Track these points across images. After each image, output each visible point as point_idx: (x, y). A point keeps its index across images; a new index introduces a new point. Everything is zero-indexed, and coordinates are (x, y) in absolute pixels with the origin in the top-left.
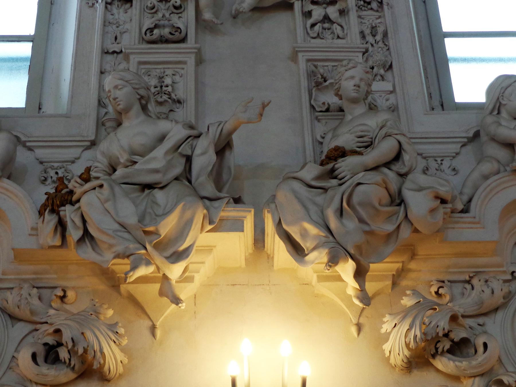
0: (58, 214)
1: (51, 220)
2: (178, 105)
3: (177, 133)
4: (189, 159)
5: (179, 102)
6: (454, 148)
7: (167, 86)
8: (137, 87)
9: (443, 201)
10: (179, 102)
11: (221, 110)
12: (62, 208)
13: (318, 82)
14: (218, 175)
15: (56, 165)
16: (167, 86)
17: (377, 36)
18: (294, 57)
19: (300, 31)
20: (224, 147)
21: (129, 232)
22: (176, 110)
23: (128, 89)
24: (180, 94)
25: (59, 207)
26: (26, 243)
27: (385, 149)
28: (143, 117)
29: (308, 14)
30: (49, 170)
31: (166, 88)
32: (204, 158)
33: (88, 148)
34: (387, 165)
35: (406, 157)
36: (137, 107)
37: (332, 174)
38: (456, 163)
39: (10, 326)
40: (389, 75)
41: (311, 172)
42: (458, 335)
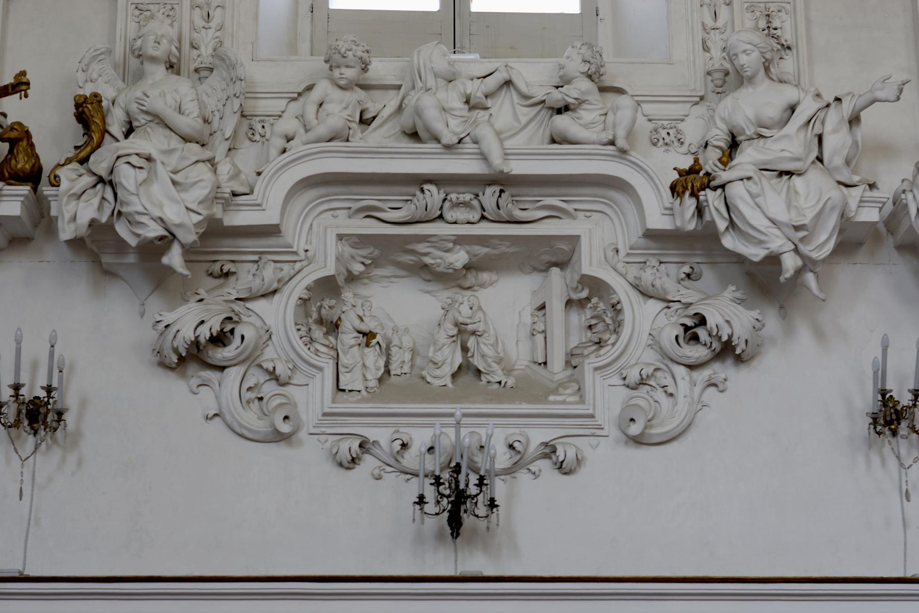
0: (698, 199)
1: (690, 204)
2: (787, 51)
4: (820, 138)
5: (789, 48)
7: (776, 29)
8: (764, 50)
10: (789, 48)
12: (702, 193)
15: (665, 123)
16: (776, 29)
21: (779, 229)
22: (785, 57)
25: (699, 191)
26: (658, 221)
28: (767, 82)
30: (660, 130)
31: (775, 32)
33: (697, 103)
36: (762, 72)
39: (642, 302)
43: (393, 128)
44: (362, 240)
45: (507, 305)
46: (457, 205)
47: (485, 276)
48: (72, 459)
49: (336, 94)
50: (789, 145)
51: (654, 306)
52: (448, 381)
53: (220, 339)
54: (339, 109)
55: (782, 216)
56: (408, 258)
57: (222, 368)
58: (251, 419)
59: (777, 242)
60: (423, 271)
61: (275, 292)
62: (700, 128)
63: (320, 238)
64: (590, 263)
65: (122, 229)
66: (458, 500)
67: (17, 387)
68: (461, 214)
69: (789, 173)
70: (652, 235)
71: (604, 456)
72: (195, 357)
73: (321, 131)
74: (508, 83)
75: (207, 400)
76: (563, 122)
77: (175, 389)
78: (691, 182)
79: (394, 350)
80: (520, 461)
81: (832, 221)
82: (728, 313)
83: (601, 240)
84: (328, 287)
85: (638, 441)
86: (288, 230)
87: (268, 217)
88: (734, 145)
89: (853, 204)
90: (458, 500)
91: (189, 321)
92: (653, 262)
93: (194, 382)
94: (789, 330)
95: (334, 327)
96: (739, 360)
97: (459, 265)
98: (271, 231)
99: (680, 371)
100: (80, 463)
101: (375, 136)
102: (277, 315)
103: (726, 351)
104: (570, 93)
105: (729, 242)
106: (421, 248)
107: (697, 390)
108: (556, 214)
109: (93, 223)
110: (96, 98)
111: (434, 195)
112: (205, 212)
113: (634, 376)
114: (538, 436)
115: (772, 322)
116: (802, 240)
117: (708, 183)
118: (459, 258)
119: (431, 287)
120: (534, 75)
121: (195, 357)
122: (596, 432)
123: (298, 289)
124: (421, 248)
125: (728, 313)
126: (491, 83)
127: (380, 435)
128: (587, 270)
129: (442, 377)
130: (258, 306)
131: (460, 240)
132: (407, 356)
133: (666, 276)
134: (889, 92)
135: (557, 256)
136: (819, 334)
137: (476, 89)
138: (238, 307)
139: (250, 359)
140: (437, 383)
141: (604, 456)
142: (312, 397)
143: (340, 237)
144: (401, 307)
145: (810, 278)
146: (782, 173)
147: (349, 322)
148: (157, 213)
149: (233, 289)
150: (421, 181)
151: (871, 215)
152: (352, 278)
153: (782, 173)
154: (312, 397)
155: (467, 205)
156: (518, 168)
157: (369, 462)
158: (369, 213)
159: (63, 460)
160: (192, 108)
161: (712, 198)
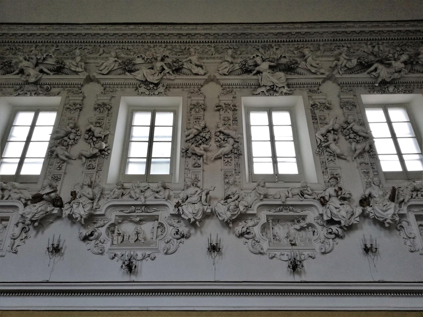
1: (177, 209)
3: (199, 191)
4: (201, 197)
6: (251, 191)
9: (246, 207)
11: (207, 186)
13: (226, 176)
14: (206, 201)
17: (238, 165)
18: (221, 170)
19: (223, 165)
20: (207, 194)
23: (190, 182)
24: (199, 179)
27: (236, 196)
29: (225, 160)
32: (204, 197)
34: (236, 200)
35: (240, 198)
37: (226, 202)
38: (251, 194)
40: (239, 174)
41: (222, 202)
42: (248, 231)
43: (128, 196)
44: (120, 216)
45: (147, 228)
46: (138, 210)
47: (144, 222)
48: (62, 258)
49: (117, 190)
50: (195, 198)
51: (172, 227)
52: (133, 242)
53: (92, 235)
54: (118, 192)
55: (191, 212)
56: (129, 219)
57: (92, 240)
58: (96, 250)
59: (190, 216)
60: (131, 221)
61: (103, 226)
62: (183, 195)
65: (74, 215)
67: (53, 245)
68: (138, 211)
69: (194, 203)
70: (171, 214)
71: (160, 256)
72: (86, 239)
73: (113, 197)
74: (149, 188)
75: (89, 246)
76: (157, 195)
77: (83, 245)
78: (178, 205)
79: (125, 236)
80: (144, 258)
81: (200, 212)
82: (184, 229)
83: (164, 215)
84: (113, 225)
85: (166, 253)
86: (107, 215)
87: (102, 212)
88: (187, 198)
89: (205, 209)
90: (130, 268)
91: (85, 232)
92: (172, 219)
93: (86, 243)
94: (196, 232)
95: (113, 232)
96: (187, 238)
97: (138, 220)
98: (103, 215)
99: (175, 240)
100: (63, 259)
101: (124, 197)
102: (103, 230)
103: (183, 236)
104: (158, 190)
105: (183, 216)
106: (131, 217)
107: (178, 244)
108: (156, 211)
109: (69, 214)
110: (75, 192)
112: (88, 212)
113: (166, 241)
114: (148, 253)
115: (193, 231)
116: (195, 216)
117: (180, 205)
118: (138, 219)
119: (134, 224)
120: (154, 186)
121: (86, 239)
122: (159, 252)
123: (107, 226)
124: (131, 217)
125: (184, 229)
126: (146, 188)
127: (119, 253)
129: (132, 241)
130: (100, 229)
131: (137, 216)
133: (174, 222)
134: (212, 189)
135: (155, 218)
136: (201, 233)
137: (143, 189)
138: (96, 229)
139: (97, 239)
140: (132, 242)
141: (160, 256)
142: (107, 246)
143: (116, 216)
144: (128, 228)
145: (197, 223)
146: (193, 203)
147: (116, 231)
148: (79, 213)
149: (95, 226)
150: (131, 205)
151: (209, 211)
152: (119, 223)
153: (193, 203)
154: (107, 246)
155: (139, 209)
156: (148, 203)
157: (116, 258)
158: (122, 211)
159: (60, 258)
160: (91, 193)
161: (180, 208)
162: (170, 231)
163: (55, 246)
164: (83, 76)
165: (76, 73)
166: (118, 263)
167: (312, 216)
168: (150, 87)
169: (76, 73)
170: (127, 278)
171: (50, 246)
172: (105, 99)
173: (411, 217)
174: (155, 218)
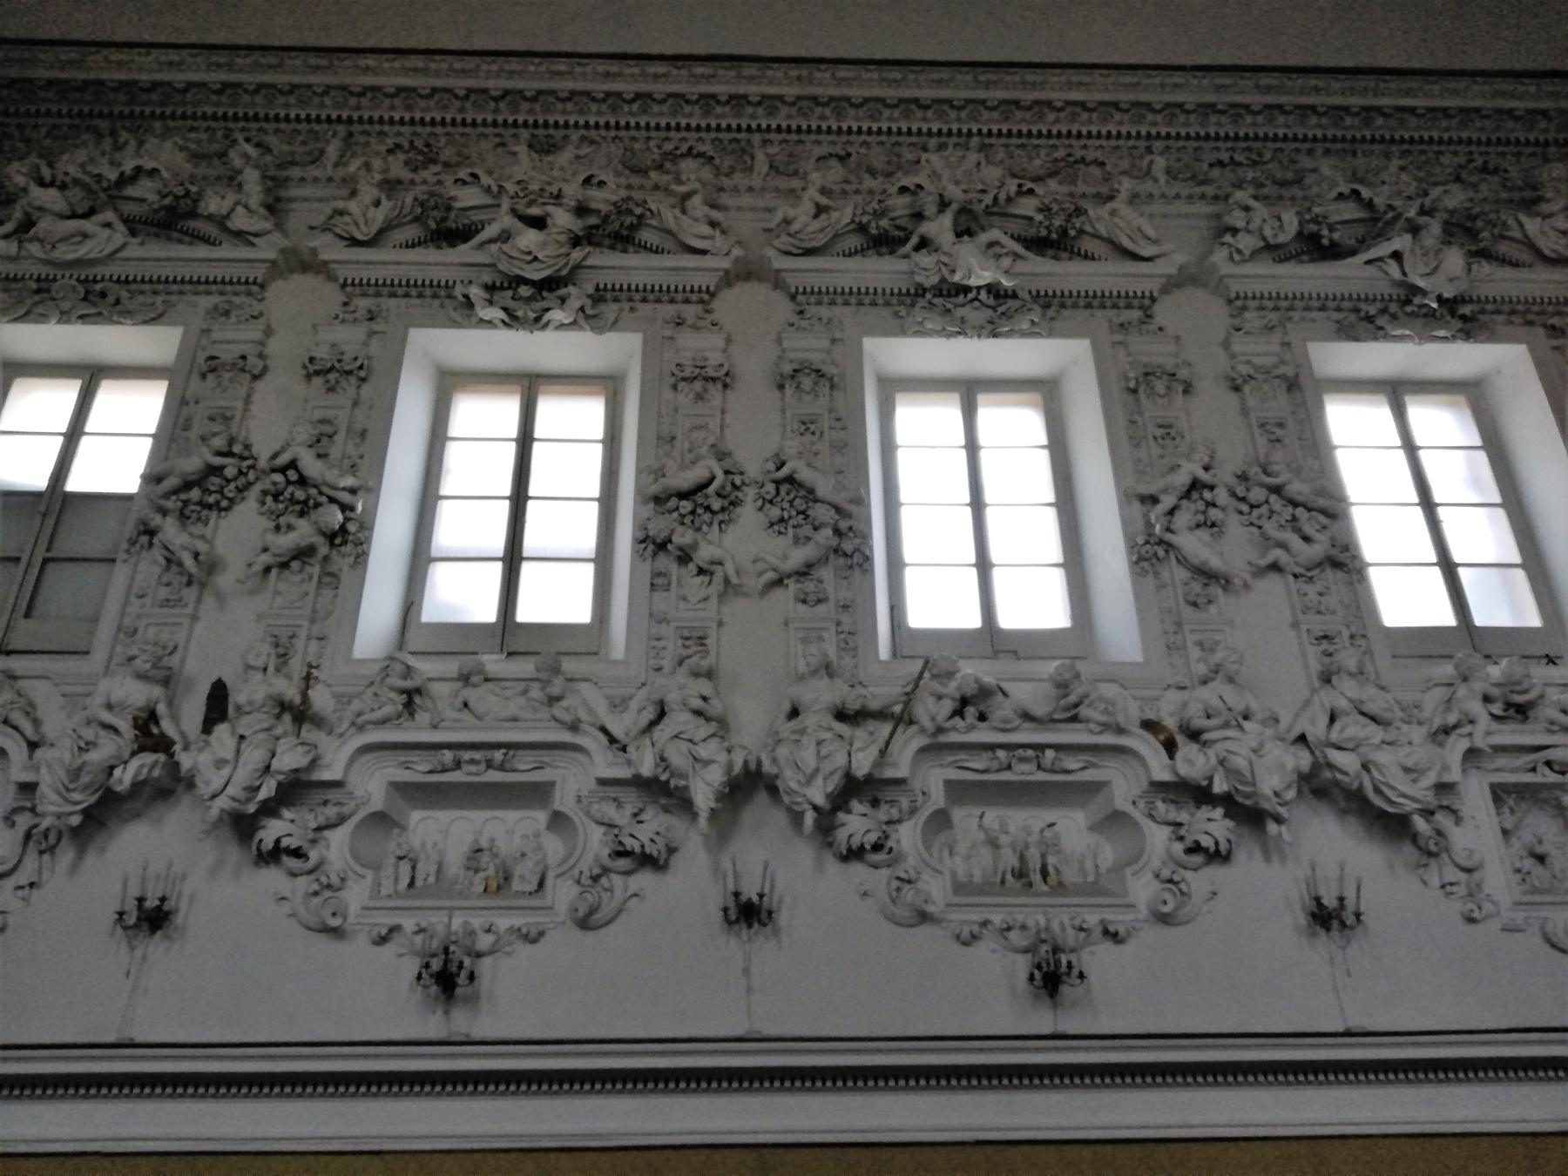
63: (372, 786)
64: (563, 800)
66: (447, 978)
70: (603, 782)
71: (564, 942)
90: (447, 978)
111: (448, 756)
128: (557, 806)
132: (433, 869)
142: (355, 896)
162: (595, 843)
163: (151, 903)
164: (266, 250)
165: (241, 236)
166: (399, 969)
167: (1123, 786)
168: (527, 297)
169: (241, 236)
170: (433, 1027)
171: (131, 905)
172: (349, 338)
173: (1475, 794)
174: (538, 793)
